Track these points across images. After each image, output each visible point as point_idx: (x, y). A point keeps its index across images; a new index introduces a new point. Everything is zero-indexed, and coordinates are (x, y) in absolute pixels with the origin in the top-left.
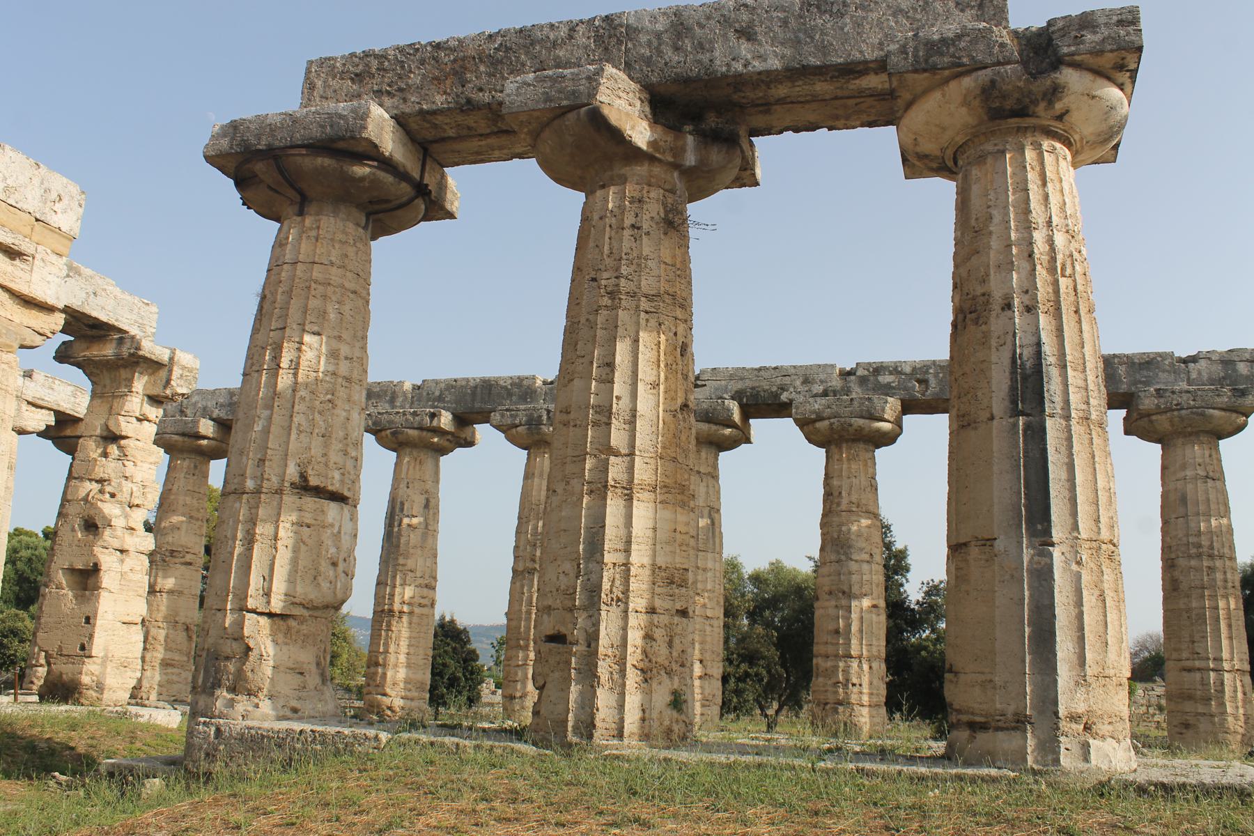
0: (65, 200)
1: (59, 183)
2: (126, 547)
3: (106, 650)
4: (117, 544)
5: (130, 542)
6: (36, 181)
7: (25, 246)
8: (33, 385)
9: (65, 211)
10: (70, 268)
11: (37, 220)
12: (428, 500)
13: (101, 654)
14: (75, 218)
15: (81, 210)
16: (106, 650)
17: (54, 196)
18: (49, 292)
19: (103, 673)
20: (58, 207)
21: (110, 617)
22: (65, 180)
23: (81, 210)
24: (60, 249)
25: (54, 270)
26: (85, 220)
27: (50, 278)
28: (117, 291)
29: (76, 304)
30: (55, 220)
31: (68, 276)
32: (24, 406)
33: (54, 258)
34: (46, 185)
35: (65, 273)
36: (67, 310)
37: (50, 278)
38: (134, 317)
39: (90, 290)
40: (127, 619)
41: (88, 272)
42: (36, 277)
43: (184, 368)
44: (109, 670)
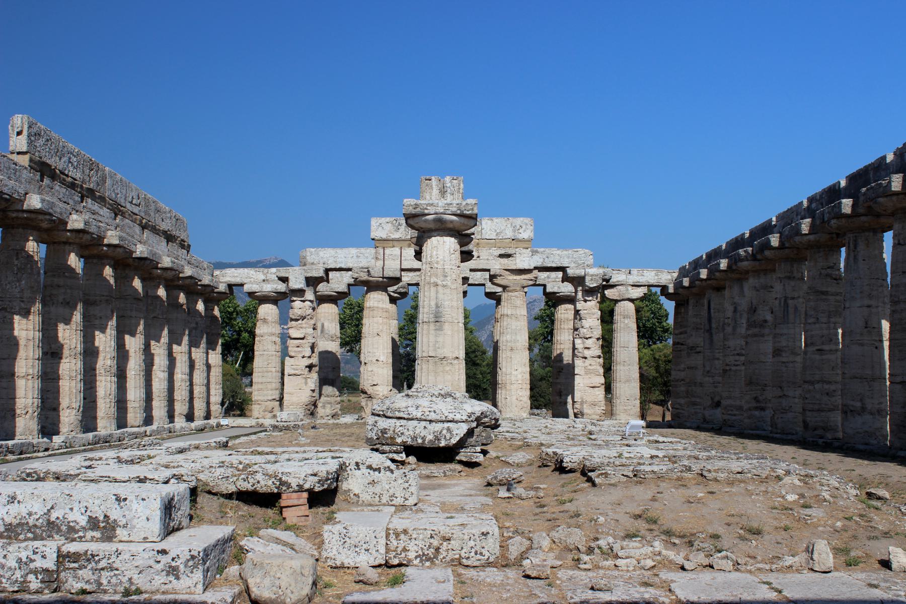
0: (524, 227)
1: (519, 221)
4: (581, 355)
5: (587, 353)
6: (509, 226)
7: (510, 251)
12: (735, 308)
16: (582, 398)
26: (535, 231)
28: (559, 252)
30: (521, 236)
32: (630, 288)
33: (524, 251)
41: (542, 250)
42: (518, 261)
43: (592, 275)
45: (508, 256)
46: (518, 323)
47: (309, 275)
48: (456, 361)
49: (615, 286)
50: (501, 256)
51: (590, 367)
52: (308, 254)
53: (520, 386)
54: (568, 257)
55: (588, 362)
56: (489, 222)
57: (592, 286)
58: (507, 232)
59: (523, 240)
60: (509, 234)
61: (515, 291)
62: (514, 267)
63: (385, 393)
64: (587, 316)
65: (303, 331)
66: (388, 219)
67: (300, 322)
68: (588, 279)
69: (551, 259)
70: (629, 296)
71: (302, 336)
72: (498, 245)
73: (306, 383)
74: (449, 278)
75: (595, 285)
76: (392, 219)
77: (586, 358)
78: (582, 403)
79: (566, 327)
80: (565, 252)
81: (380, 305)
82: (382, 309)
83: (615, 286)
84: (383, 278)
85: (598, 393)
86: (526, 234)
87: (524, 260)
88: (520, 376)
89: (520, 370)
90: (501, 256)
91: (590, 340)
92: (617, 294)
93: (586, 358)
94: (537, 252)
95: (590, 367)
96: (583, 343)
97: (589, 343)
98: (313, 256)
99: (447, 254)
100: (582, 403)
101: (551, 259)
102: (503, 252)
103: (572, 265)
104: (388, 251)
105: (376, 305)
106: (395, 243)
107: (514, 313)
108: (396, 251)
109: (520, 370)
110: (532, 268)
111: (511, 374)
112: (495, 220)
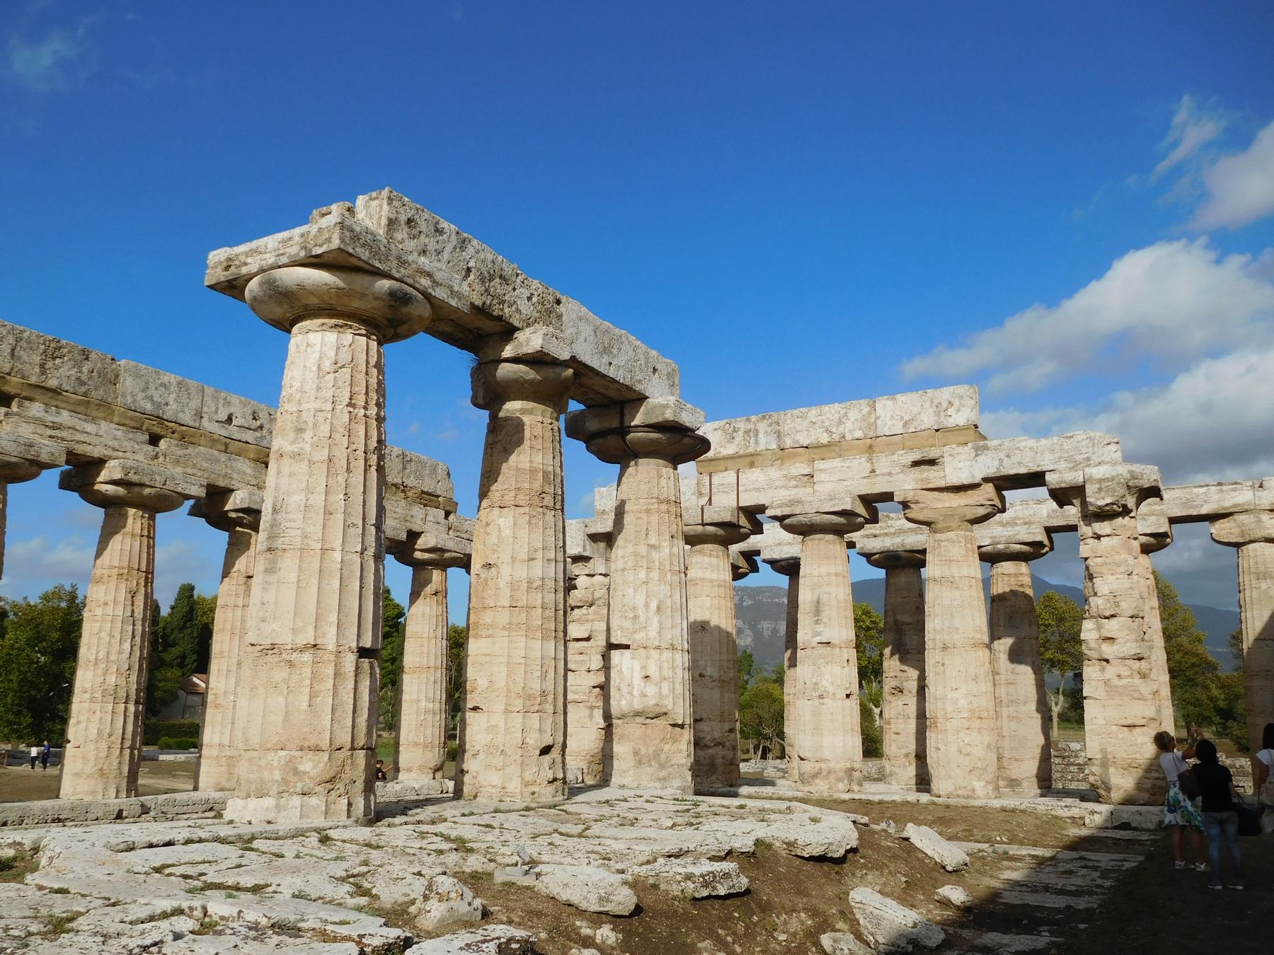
0: (956, 403)
2: (1106, 657)
3: (1103, 751)
5: (1107, 650)
6: (927, 405)
7: (932, 454)
8: (1265, 493)
9: (958, 410)
10: (977, 449)
13: (1100, 756)
15: (973, 402)
16: (1103, 751)
17: (945, 405)
18: (963, 476)
19: (1107, 774)
20: (950, 412)
21: (1101, 721)
22: (951, 388)
23: (973, 402)
24: (964, 439)
25: (962, 457)
27: (960, 465)
28: (1032, 443)
29: (992, 471)
30: (951, 423)
33: (960, 449)
34: (936, 402)
36: (986, 480)
37: (960, 465)
38: (1057, 455)
39: (1002, 455)
40: (1129, 722)
42: (948, 470)
43: (1100, 481)
44: (1112, 770)
45: (932, 462)
46: (957, 593)
47: (593, 531)
48: (307, 657)
49: (1231, 514)
50: (916, 464)
51: (1116, 681)
52: (597, 497)
53: (966, 724)
54: (1052, 451)
55: (1111, 671)
56: (889, 403)
57: (1101, 503)
58: (925, 418)
59: (957, 429)
60: (928, 420)
61: (949, 529)
62: (942, 484)
63: (717, 735)
64: (1104, 570)
65: (588, 626)
66: (716, 424)
67: (584, 610)
68: (1090, 490)
69: (1015, 459)
70: (1265, 533)
71: (586, 636)
72: (907, 443)
73: (591, 716)
74: (308, 435)
75: (1109, 500)
76: (722, 423)
77: (1107, 661)
78: (1105, 764)
80: (1044, 442)
81: (707, 575)
82: (711, 581)
83: (1231, 514)
84: (703, 525)
85: (1140, 739)
86: (960, 417)
87: (962, 465)
88: (963, 703)
89: (963, 690)
90: (916, 464)
91: (1114, 621)
92: (1236, 531)
94: (986, 448)
95: (1116, 681)
96: (1099, 628)
97: (1111, 627)
98: (604, 500)
99: (311, 376)
100: (1105, 764)
101: (1015, 459)
102: (917, 456)
103: (1063, 465)
104: (716, 479)
105: (699, 575)
106: (729, 463)
107: (947, 573)
108: (730, 477)
109: (963, 690)
110: (977, 480)
111: (945, 697)
112: (901, 398)
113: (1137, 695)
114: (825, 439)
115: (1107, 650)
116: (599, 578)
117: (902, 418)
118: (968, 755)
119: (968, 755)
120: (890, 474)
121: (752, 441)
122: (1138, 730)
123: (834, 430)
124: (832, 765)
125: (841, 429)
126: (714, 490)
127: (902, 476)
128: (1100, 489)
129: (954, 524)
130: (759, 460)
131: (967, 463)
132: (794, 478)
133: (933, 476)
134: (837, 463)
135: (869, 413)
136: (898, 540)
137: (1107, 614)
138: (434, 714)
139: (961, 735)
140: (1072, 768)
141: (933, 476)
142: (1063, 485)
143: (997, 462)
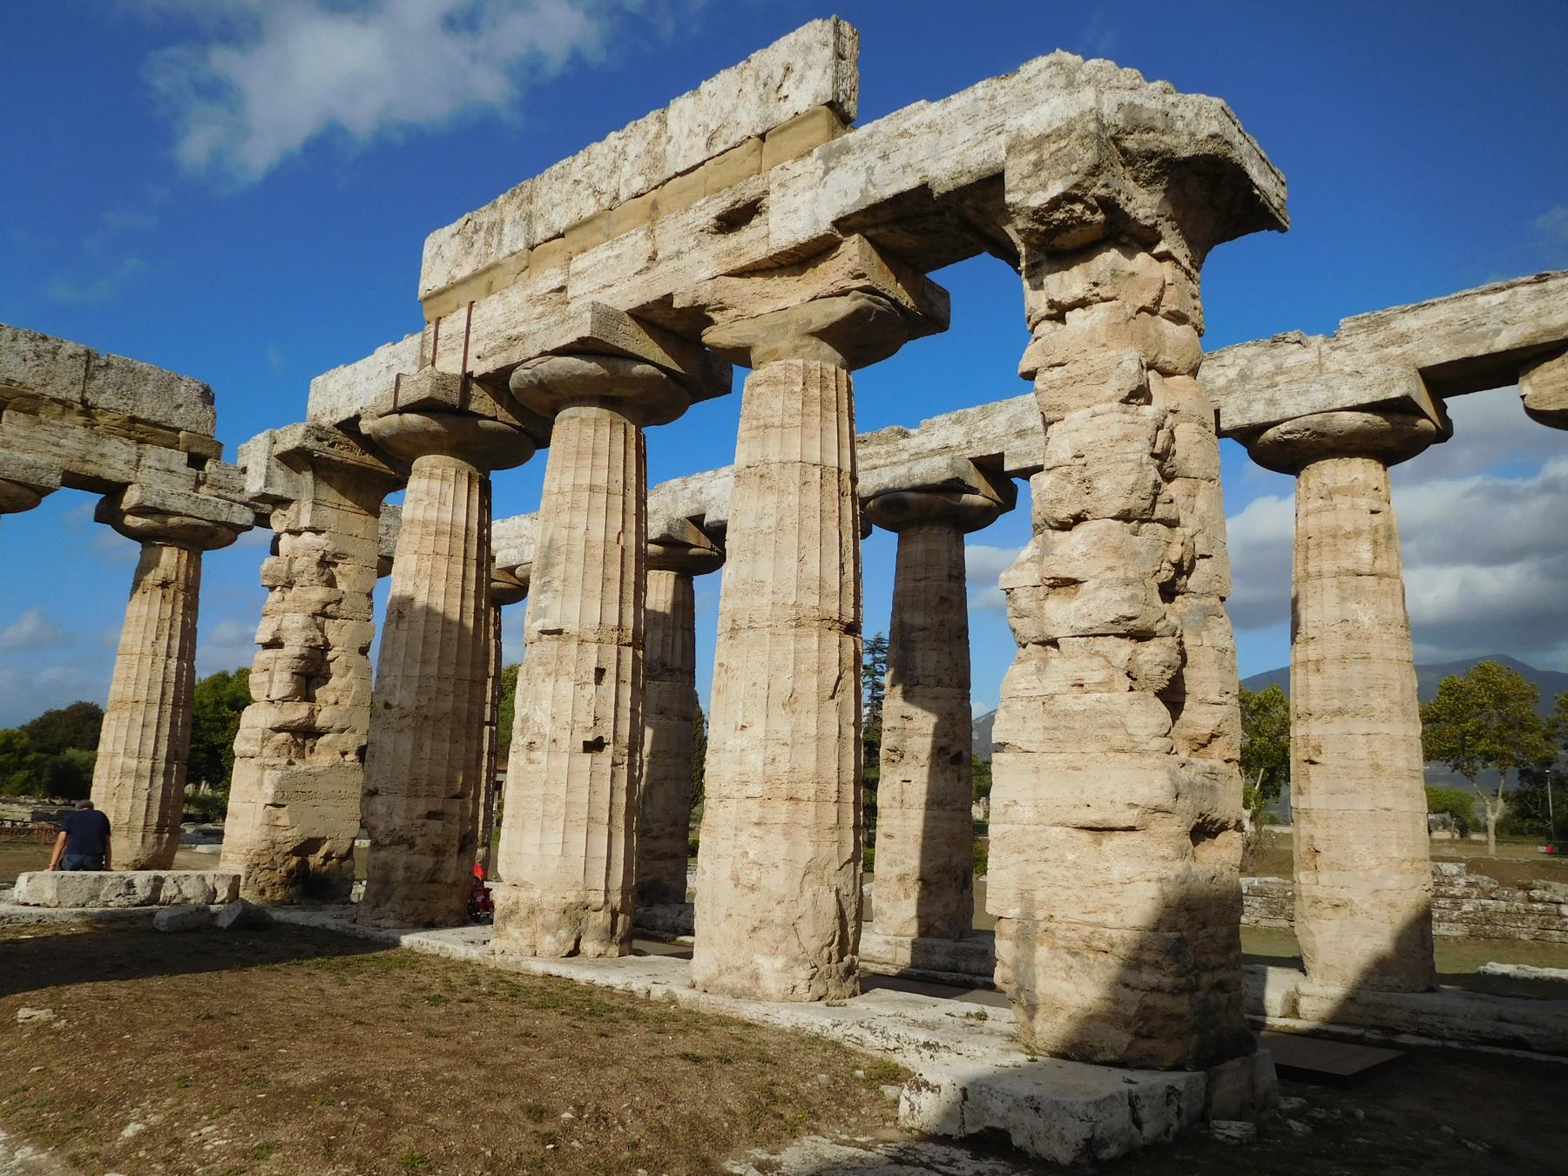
0: (798, 66)
2: (1053, 632)
3: (1026, 897)
6: (748, 88)
7: (749, 192)
10: (826, 157)
11: (762, 137)
13: (1014, 912)
14: (820, 72)
16: (1026, 897)
19: (1030, 964)
21: (1026, 813)
25: (800, 184)
27: (797, 202)
31: (826, 173)
33: (798, 168)
34: (763, 75)
35: (820, 173)
36: (845, 225)
37: (797, 202)
38: (980, 126)
40: (1092, 817)
43: (1039, 142)
44: (1042, 952)
51: (1071, 701)
54: (972, 118)
55: (1062, 668)
60: (749, 120)
63: (398, 821)
69: (897, 160)
73: (260, 783)
75: (1056, 189)
77: (1054, 643)
79: (1328, 566)
85: (1121, 869)
88: (755, 760)
89: (758, 730)
93: (1054, 643)
95: (1071, 701)
97: (1072, 551)
109: (758, 730)
110: (824, 227)
113: (1118, 739)
114: (590, 207)
115: (1061, 613)
116: (308, 537)
117: (707, 126)
118: (752, 888)
119: (752, 888)
120: (679, 253)
121: (495, 243)
122: (1118, 840)
123: (603, 187)
124: (536, 894)
125: (613, 182)
126: (440, 349)
127: (696, 254)
128: (1038, 165)
129: (784, 345)
130: (498, 277)
131: (809, 195)
132: (542, 299)
133: (754, 242)
134: (601, 253)
135: (658, 136)
136: (902, 471)
137: (1063, 513)
138: (139, 776)
139: (744, 838)
140: (1441, 902)
141: (754, 242)
142: (964, 180)
143: (862, 177)
